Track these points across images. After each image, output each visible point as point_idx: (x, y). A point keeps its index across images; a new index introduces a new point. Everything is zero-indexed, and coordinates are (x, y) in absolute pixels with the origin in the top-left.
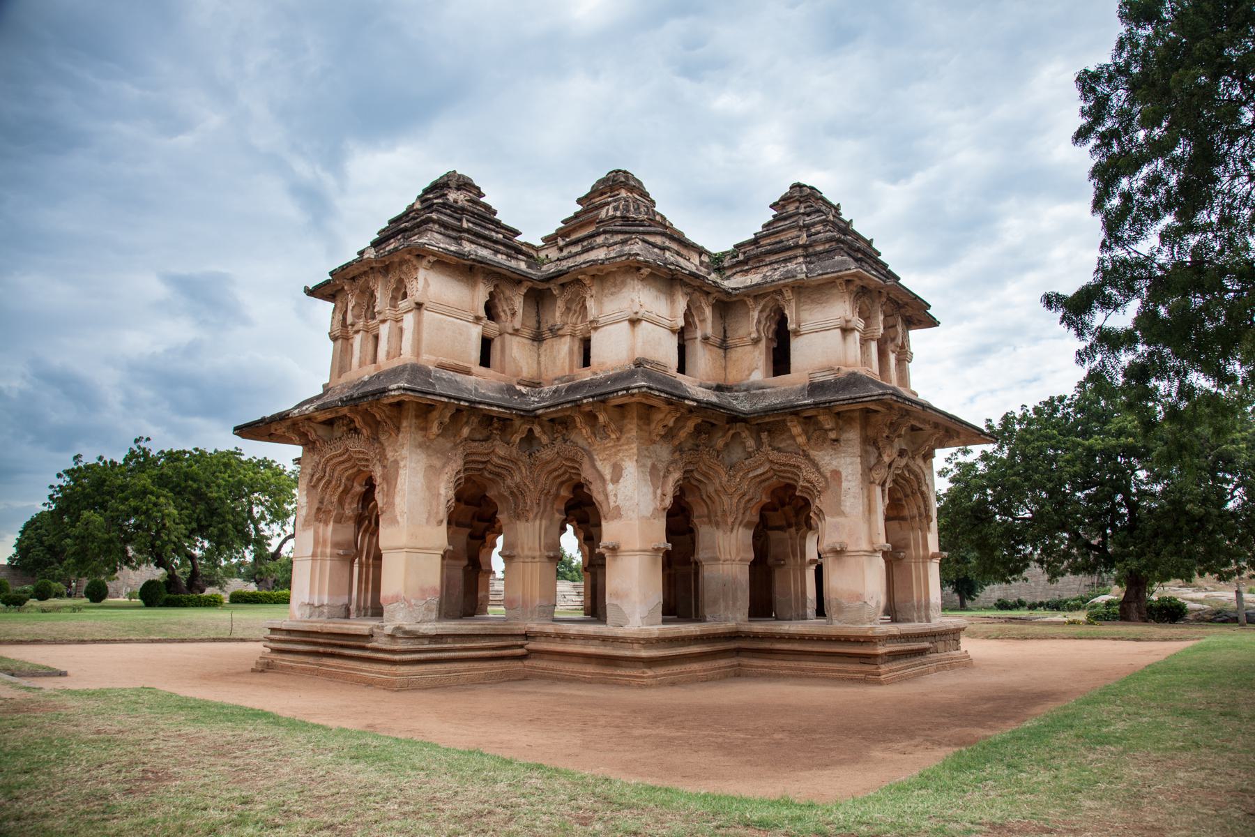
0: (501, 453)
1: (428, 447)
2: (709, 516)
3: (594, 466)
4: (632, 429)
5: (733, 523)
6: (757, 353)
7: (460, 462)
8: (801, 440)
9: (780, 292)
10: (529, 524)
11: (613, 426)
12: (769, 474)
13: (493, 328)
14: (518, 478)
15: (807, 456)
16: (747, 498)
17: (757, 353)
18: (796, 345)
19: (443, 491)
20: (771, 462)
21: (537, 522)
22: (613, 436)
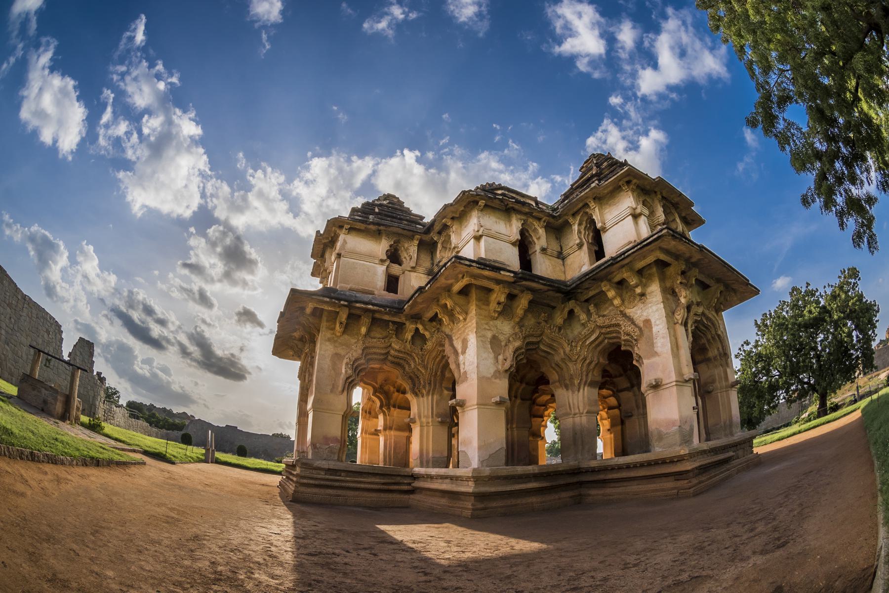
0: (397, 347)
1: (335, 342)
2: (559, 381)
3: (452, 345)
4: (473, 310)
5: (580, 384)
6: (583, 254)
7: (360, 352)
8: (617, 302)
9: (586, 205)
10: (425, 398)
11: (458, 309)
12: (600, 339)
13: (396, 269)
14: (413, 366)
15: (624, 315)
16: (588, 361)
17: (583, 254)
18: (606, 238)
19: (343, 371)
20: (600, 327)
21: (430, 397)
22: (461, 318)
